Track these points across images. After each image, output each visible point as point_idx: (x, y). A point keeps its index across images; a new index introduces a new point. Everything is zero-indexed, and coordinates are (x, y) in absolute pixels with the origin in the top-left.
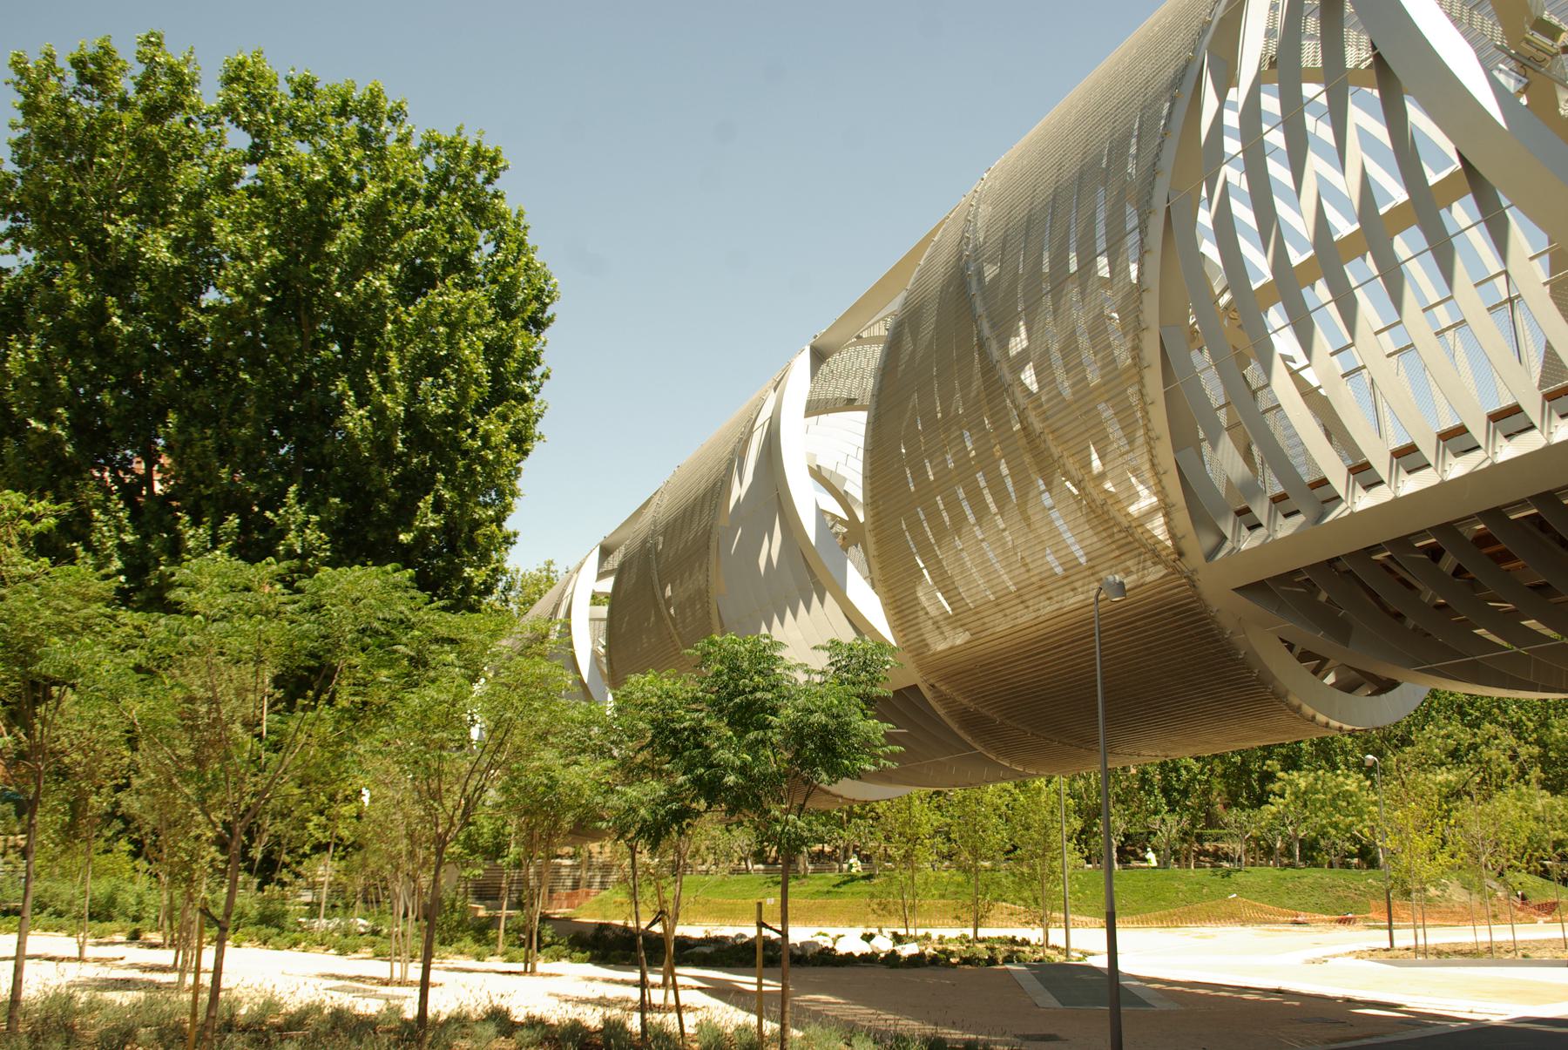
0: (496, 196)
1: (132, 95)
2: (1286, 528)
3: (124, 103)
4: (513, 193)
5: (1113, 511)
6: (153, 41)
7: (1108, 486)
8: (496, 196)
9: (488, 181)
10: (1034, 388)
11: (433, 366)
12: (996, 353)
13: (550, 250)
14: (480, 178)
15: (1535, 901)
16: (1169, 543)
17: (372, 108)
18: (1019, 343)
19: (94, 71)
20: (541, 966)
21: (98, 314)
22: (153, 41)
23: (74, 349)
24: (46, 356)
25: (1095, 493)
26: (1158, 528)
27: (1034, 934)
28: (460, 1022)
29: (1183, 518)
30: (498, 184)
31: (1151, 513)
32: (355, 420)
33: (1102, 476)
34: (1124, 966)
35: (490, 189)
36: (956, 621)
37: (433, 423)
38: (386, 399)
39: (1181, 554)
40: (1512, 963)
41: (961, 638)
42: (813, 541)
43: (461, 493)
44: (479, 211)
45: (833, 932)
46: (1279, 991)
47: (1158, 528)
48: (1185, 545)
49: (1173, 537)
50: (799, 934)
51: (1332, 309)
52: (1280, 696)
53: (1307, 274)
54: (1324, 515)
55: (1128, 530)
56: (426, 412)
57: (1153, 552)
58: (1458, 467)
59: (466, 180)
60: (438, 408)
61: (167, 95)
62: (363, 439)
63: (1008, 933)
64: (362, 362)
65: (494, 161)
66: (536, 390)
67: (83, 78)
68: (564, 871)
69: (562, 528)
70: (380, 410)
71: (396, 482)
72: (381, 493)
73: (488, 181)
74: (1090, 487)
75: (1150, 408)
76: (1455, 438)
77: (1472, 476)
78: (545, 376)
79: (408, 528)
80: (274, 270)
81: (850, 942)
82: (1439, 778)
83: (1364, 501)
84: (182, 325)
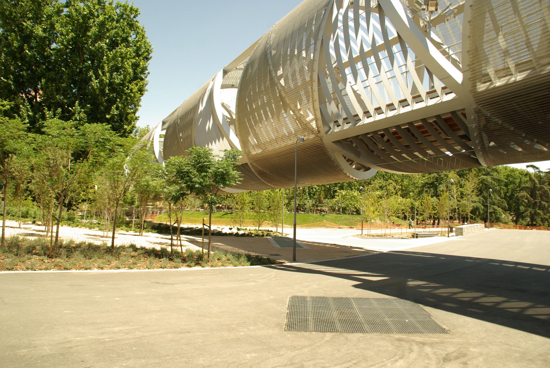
0: (136, 22)
2: (346, 127)
4: (141, 21)
5: (302, 120)
7: (301, 112)
8: (136, 22)
9: (134, 17)
10: (283, 85)
11: (116, 69)
12: (274, 75)
14: (132, 16)
15: (396, 223)
18: (280, 72)
20: (144, 234)
21: (21, 49)
23: (15, 58)
24: (6, 60)
25: (298, 114)
26: (314, 124)
27: (274, 229)
28: (123, 248)
29: (320, 122)
30: (137, 19)
31: (312, 120)
32: (95, 83)
33: (300, 110)
34: (297, 238)
35: (135, 19)
36: (258, 146)
37: (116, 85)
38: (104, 78)
39: (319, 132)
40: (389, 238)
41: (260, 151)
43: (124, 105)
44: (131, 26)
45: (221, 227)
47: (314, 124)
48: (320, 129)
49: (317, 127)
50: (213, 228)
51: (375, 64)
52: (341, 170)
53: (369, 54)
55: (306, 125)
56: (115, 82)
57: (312, 131)
58: (391, 114)
60: (117, 81)
63: (267, 229)
64: (98, 67)
65: (136, 11)
68: (150, 209)
69: (152, 115)
71: (106, 101)
72: (102, 104)
73: (134, 17)
74: (296, 112)
76: (390, 106)
77: (393, 116)
78: (149, 73)
79: (109, 114)
80: (72, 39)
81: (226, 230)
82: (377, 193)
83: (367, 121)
84: (46, 53)
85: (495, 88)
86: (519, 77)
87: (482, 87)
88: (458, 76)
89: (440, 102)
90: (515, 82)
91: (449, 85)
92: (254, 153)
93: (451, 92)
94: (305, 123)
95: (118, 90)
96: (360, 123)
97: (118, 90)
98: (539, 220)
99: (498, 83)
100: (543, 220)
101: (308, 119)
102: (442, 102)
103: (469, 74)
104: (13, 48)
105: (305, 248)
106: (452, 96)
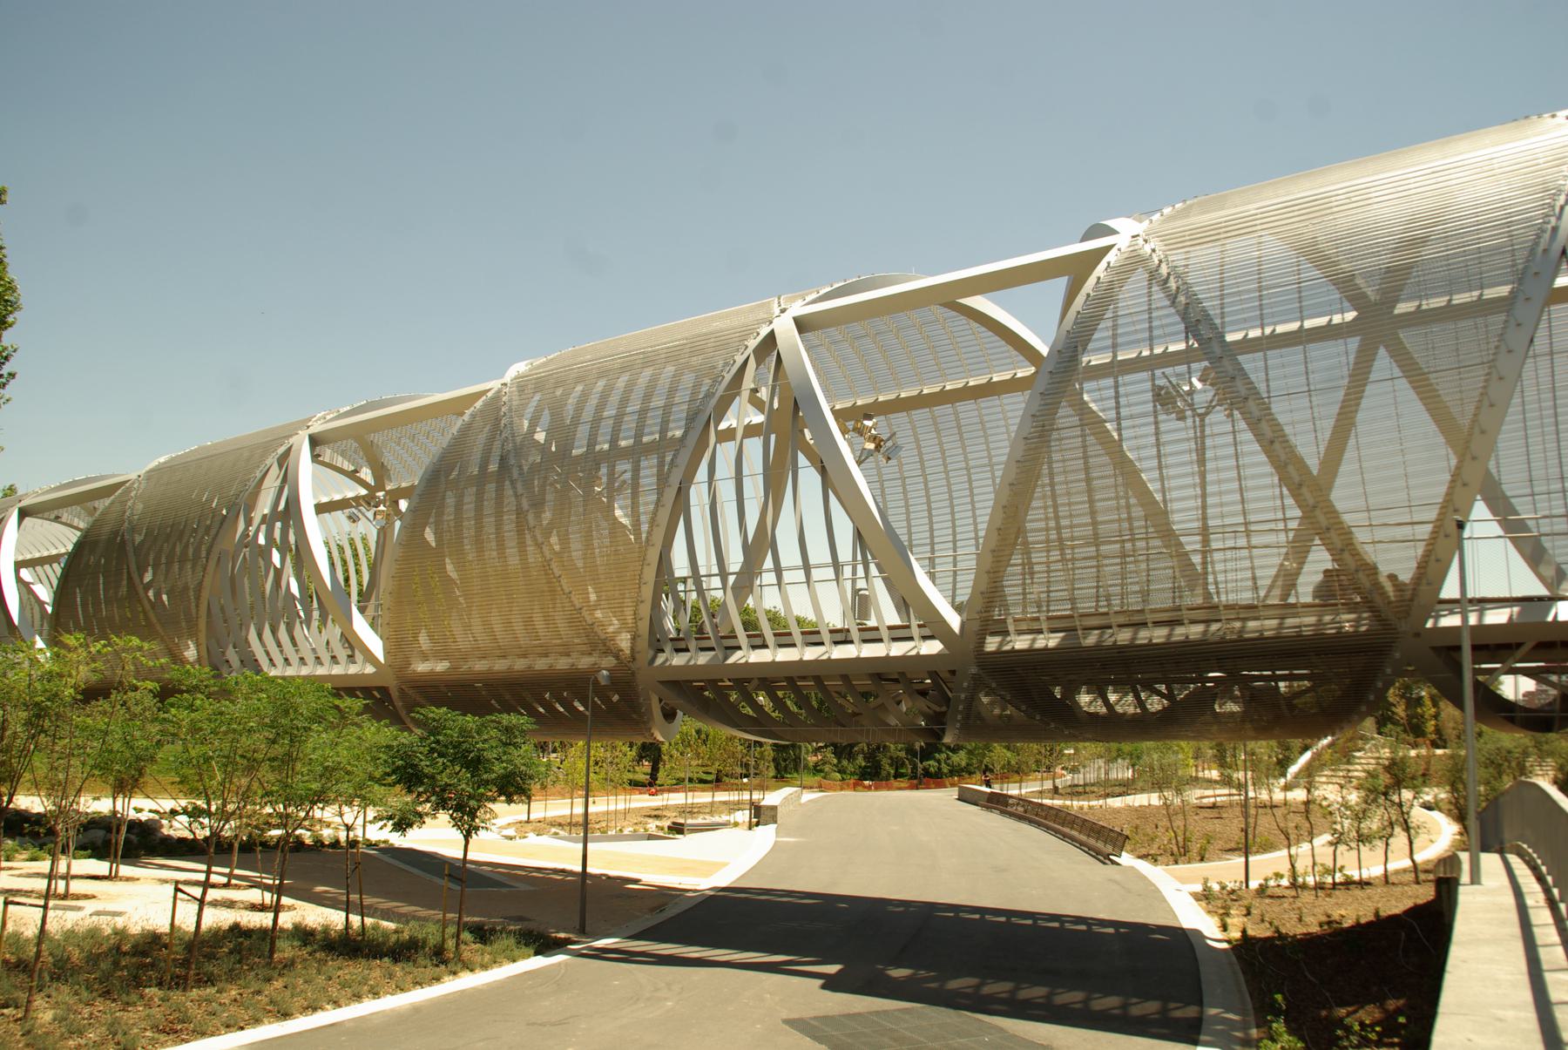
2: (703, 659)
7: (598, 614)
10: (557, 548)
16: (628, 652)
20: (125, 870)
25: (588, 618)
26: (624, 641)
29: (643, 643)
31: (618, 632)
34: (469, 857)
36: (440, 655)
39: (634, 659)
41: (441, 666)
46: (563, 871)
47: (624, 641)
49: (632, 649)
54: (726, 658)
74: (585, 613)
75: (644, 588)
78: (12, 375)
85: (1013, 651)
86: (1053, 641)
87: (992, 644)
88: (954, 621)
89: (913, 653)
90: (1046, 649)
91: (934, 627)
92: (422, 667)
93: (931, 637)
96: (735, 658)
98: (885, 763)
99: (1021, 643)
100: (897, 764)
101: (611, 629)
102: (918, 655)
103: (976, 626)
105: (522, 887)
106: (933, 647)
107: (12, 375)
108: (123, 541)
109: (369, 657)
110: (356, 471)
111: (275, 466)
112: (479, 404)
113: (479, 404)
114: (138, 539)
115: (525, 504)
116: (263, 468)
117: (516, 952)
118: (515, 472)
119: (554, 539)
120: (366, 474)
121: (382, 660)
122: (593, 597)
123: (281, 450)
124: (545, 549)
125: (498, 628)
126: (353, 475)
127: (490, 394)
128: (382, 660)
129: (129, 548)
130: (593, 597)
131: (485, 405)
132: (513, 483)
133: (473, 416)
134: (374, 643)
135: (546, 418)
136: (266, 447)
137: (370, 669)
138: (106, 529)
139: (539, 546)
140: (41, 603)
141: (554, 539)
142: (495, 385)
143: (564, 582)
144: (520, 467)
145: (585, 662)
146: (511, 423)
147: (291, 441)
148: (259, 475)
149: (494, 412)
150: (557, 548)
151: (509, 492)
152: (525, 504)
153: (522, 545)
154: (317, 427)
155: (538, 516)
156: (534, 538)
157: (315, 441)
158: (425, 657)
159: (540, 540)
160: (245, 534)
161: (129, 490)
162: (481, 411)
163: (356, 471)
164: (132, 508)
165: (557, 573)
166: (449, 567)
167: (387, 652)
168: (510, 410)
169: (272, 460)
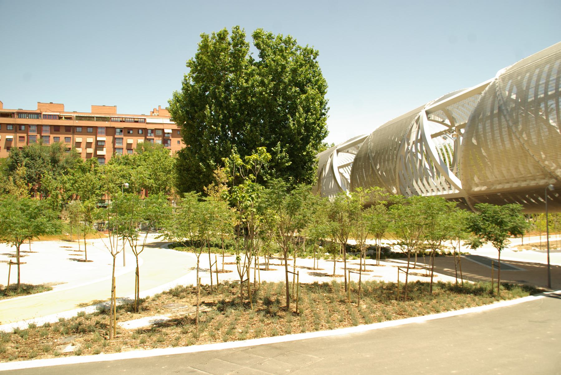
0: (316, 62)
1: (231, 42)
3: (229, 44)
5: (546, 169)
6: (237, 28)
7: (546, 163)
9: (314, 59)
10: (526, 139)
12: (514, 129)
13: (324, 76)
14: (312, 57)
17: (288, 42)
19: (222, 37)
20: (381, 263)
21: (226, 99)
22: (237, 28)
30: (317, 59)
31: (556, 169)
32: (291, 123)
33: (545, 160)
35: (314, 61)
36: (483, 184)
38: (301, 119)
41: (484, 188)
42: (439, 163)
44: (312, 66)
46: (539, 264)
55: (550, 173)
59: (309, 58)
60: (311, 121)
61: (239, 40)
62: (294, 129)
64: (293, 110)
65: (317, 54)
66: (327, 112)
67: (220, 38)
70: (299, 122)
71: (302, 139)
72: (298, 142)
73: (314, 59)
74: (541, 163)
78: (329, 108)
79: (305, 150)
92: (476, 189)
94: (549, 171)
95: (309, 128)
97: (309, 128)
101: (552, 168)
104: (221, 99)
105: (523, 270)
107: (329, 108)
108: (369, 157)
109: (457, 187)
110: (443, 121)
111: (415, 124)
112: (487, 88)
113: (487, 88)
114: (373, 155)
115: (511, 124)
116: (411, 125)
117: (522, 294)
118: (505, 112)
119: (524, 136)
120: (447, 122)
121: (461, 188)
122: (543, 156)
123: (416, 118)
124: (521, 140)
125: (505, 172)
126: (442, 123)
127: (491, 84)
128: (461, 188)
129: (371, 158)
130: (543, 156)
131: (490, 88)
132: (505, 116)
133: (485, 93)
134: (458, 182)
135: (515, 89)
136: (411, 118)
137: (457, 191)
138: (363, 153)
139: (518, 139)
140: (346, 179)
141: (524, 136)
142: (492, 80)
143: (530, 152)
144: (507, 109)
145: (542, 182)
146: (501, 93)
147: (419, 114)
148: (410, 127)
149: (494, 91)
150: (526, 139)
151: (503, 120)
152: (511, 124)
153: (511, 139)
154: (428, 108)
155: (517, 128)
156: (516, 136)
157: (427, 113)
158: (477, 185)
159: (518, 136)
160: (408, 149)
161: (368, 139)
162: (488, 91)
163: (443, 121)
164: (370, 145)
165: (527, 148)
166: (483, 151)
167: (463, 185)
168: (500, 88)
169: (414, 122)
